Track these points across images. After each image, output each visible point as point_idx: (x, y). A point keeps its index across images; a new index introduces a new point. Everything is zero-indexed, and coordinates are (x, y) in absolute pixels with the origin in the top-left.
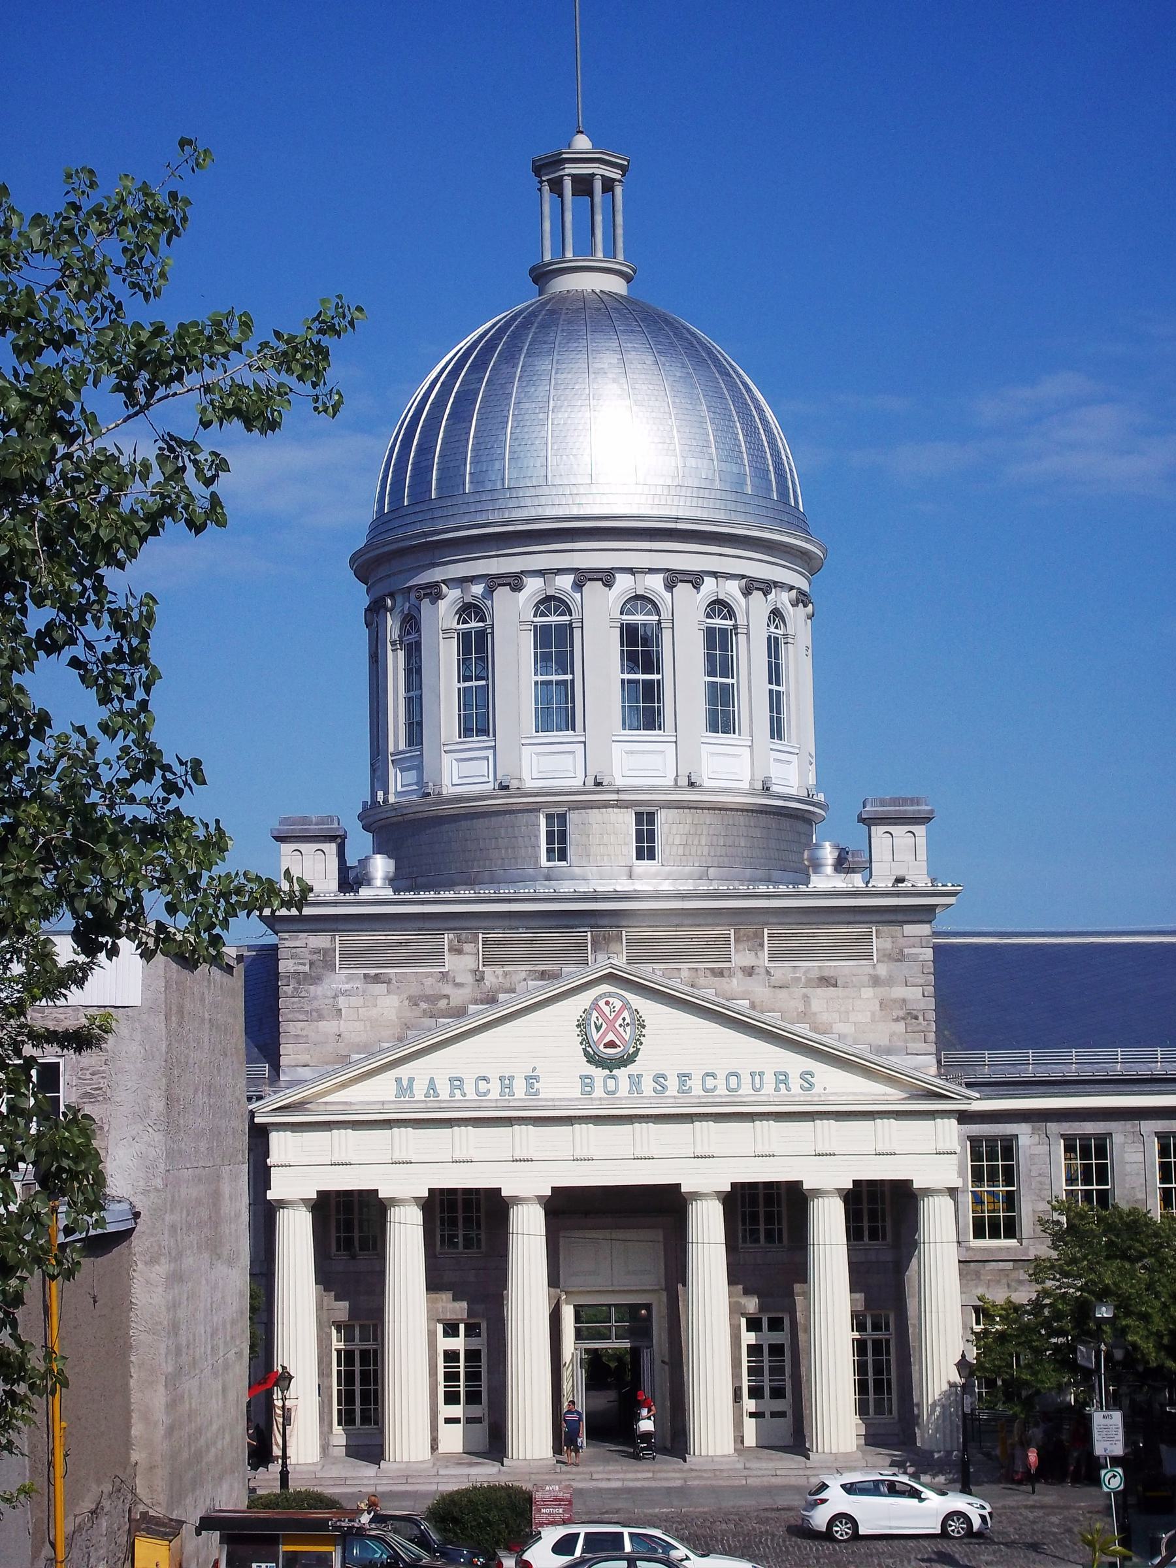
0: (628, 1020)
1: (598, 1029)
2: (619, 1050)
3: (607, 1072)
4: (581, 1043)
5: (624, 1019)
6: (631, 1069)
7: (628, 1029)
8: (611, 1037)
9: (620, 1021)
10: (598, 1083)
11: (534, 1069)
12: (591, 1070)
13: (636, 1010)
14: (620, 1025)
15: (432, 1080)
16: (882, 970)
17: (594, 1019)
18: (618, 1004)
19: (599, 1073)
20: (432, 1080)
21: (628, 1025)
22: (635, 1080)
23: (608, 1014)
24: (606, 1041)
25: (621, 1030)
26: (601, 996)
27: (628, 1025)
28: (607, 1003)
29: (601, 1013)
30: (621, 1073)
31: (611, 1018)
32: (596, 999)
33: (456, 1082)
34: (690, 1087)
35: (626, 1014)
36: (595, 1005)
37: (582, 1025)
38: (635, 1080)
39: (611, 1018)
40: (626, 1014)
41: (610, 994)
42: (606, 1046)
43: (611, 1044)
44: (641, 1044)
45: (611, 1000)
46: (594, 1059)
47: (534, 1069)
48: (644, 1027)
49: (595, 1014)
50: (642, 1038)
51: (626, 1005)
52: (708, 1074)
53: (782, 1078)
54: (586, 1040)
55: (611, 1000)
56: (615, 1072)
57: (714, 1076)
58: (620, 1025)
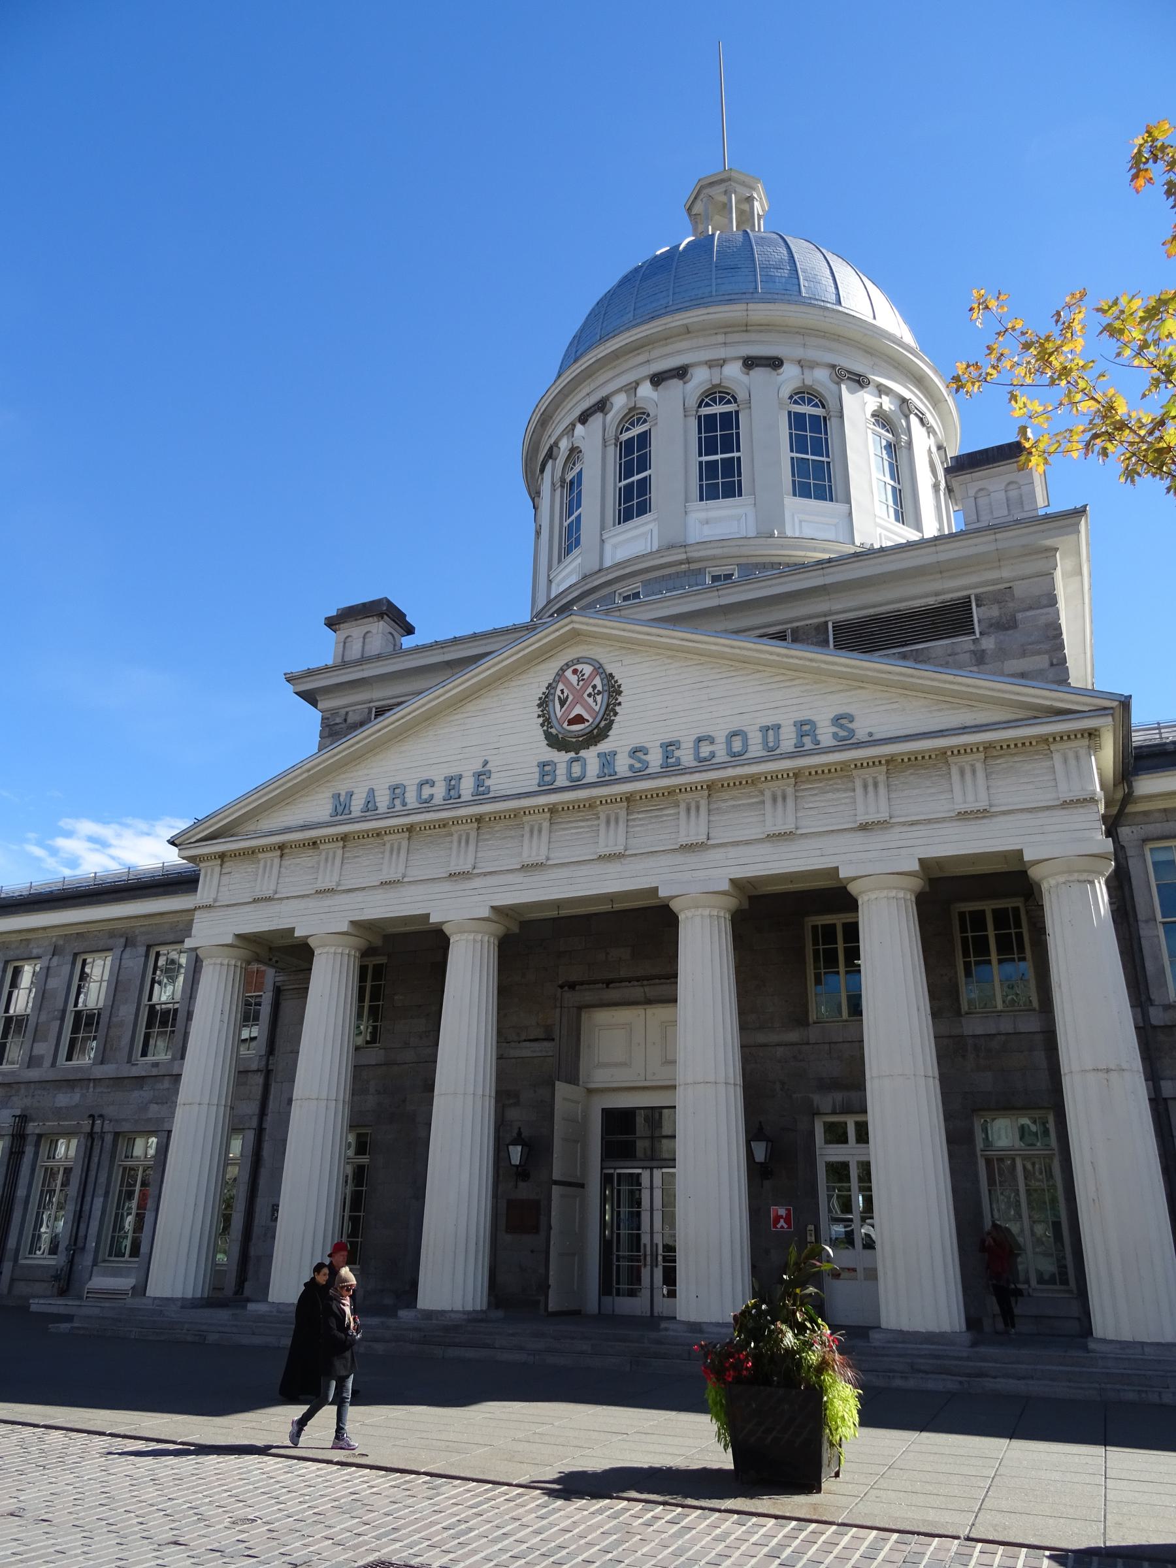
0: (599, 688)
1: (563, 703)
2: (587, 724)
3: (572, 754)
4: (542, 725)
5: (594, 687)
6: (604, 746)
7: (599, 698)
8: (578, 710)
9: (590, 690)
10: (561, 770)
11: (486, 763)
13: (611, 675)
14: (589, 695)
15: (372, 791)
16: (988, 643)
17: (558, 693)
18: (587, 670)
19: (561, 758)
20: (372, 791)
21: (599, 693)
22: (607, 760)
23: (575, 683)
24: (572, 716)
25: (590, 700)
26: (567, 665)
27: (599, 693)
28: (575, 672)
29: (568, 683)
30: (590, 755)
31: (578, 688)
32: (563, 670)
33: (397, 791)
34: (678, 758)
35: (597, 681)
36: (560, 675)
37: (544, 703)
38: (607, 760)
39: (578, 688)
41: (579, 661)
42: (571, 722)
43: (579, 719)
44: (616, 714)
45: (579, 667)
46: (556, 742)
47: (486, 763)
48: (620, 693)
49: (561, 686)
50: (617, 708)
51: (599, 669)
52: (699, 740)
53: (805, 728)
54: (547, 722)
55: (579, 667)
56: (583, 753)
57: (711, 740)
58: (589, 695)
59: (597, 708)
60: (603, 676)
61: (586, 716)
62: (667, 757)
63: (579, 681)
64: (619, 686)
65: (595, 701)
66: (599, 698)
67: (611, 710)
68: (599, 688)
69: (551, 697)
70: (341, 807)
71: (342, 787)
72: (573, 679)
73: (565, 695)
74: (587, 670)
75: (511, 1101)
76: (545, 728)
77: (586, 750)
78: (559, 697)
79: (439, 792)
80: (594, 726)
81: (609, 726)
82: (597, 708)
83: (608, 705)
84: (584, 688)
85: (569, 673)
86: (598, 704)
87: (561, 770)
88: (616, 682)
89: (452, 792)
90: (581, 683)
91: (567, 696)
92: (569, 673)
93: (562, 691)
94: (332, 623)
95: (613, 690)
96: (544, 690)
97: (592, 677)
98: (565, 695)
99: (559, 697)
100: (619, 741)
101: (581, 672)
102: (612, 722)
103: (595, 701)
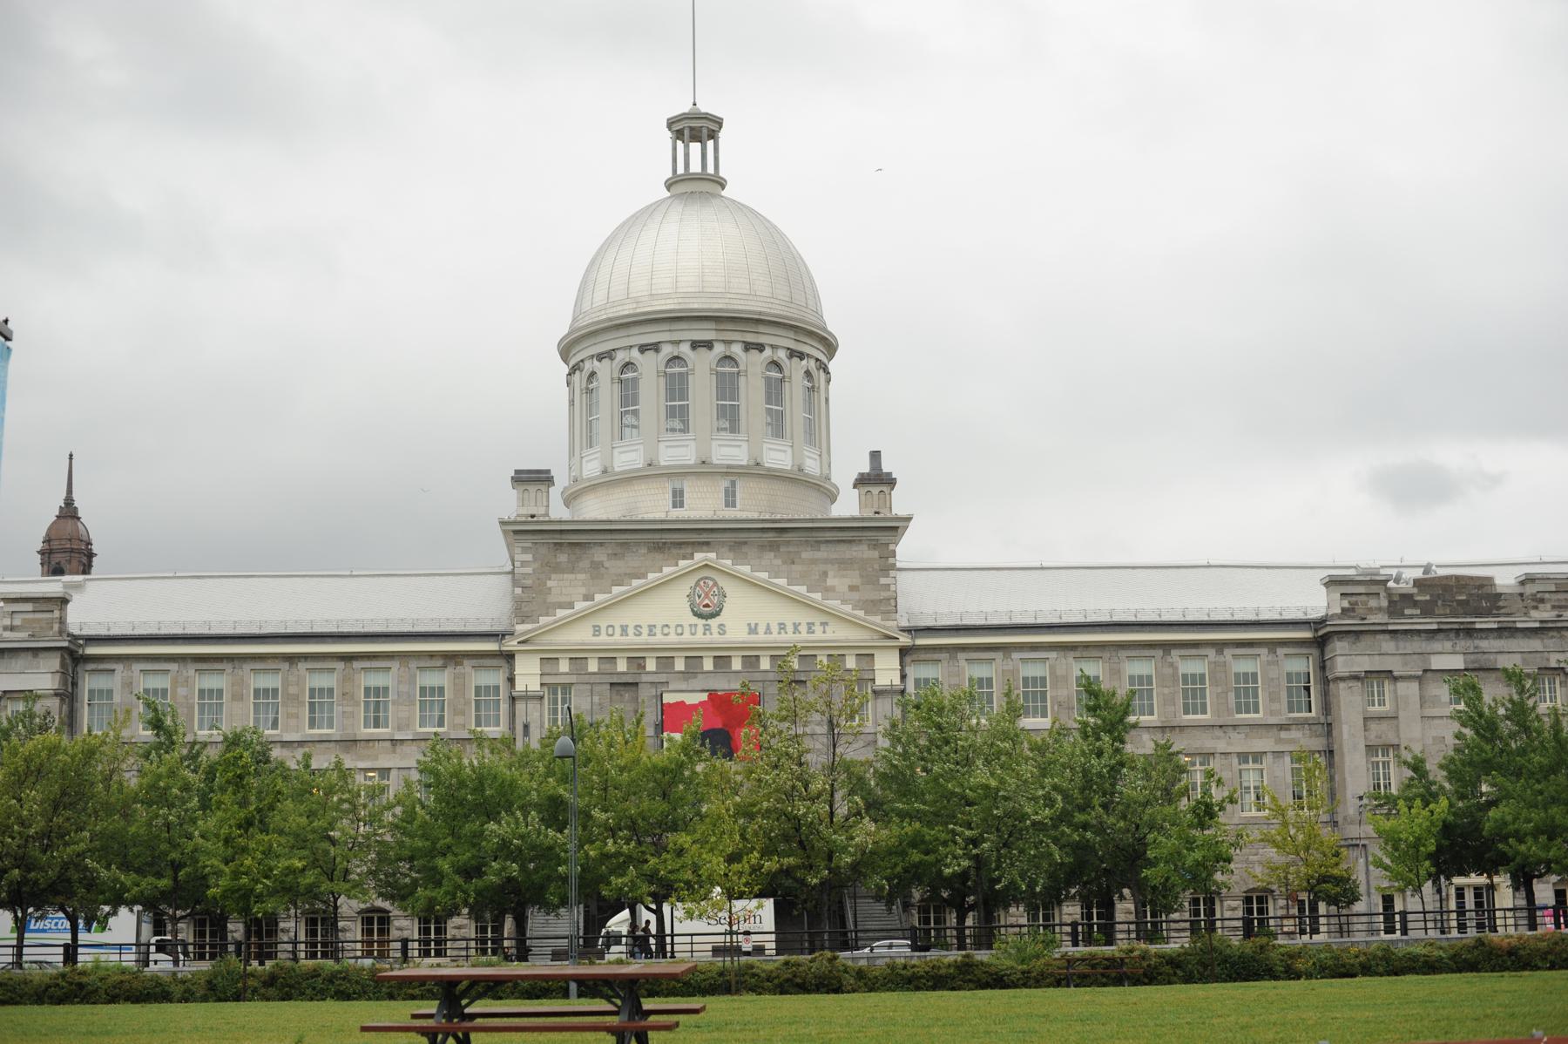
1: (699, 597)
8: (707, 601)
12: (695, 620)
18: (711, 583)
19: (701, 622)
26: (702, 579)
30: (714, 622)
35: (715, 589)
36: (697, 584)
40: (715, 589)
41: (706, 578)
43: (707, 606)
46: (696, 614)
51: (715, 584)
74: (711, 583)
81: (721, 610)
84: (710, 591)
85: (702, 583)
87: (700, 629)
92: (702, 583)
97: (713, 586)
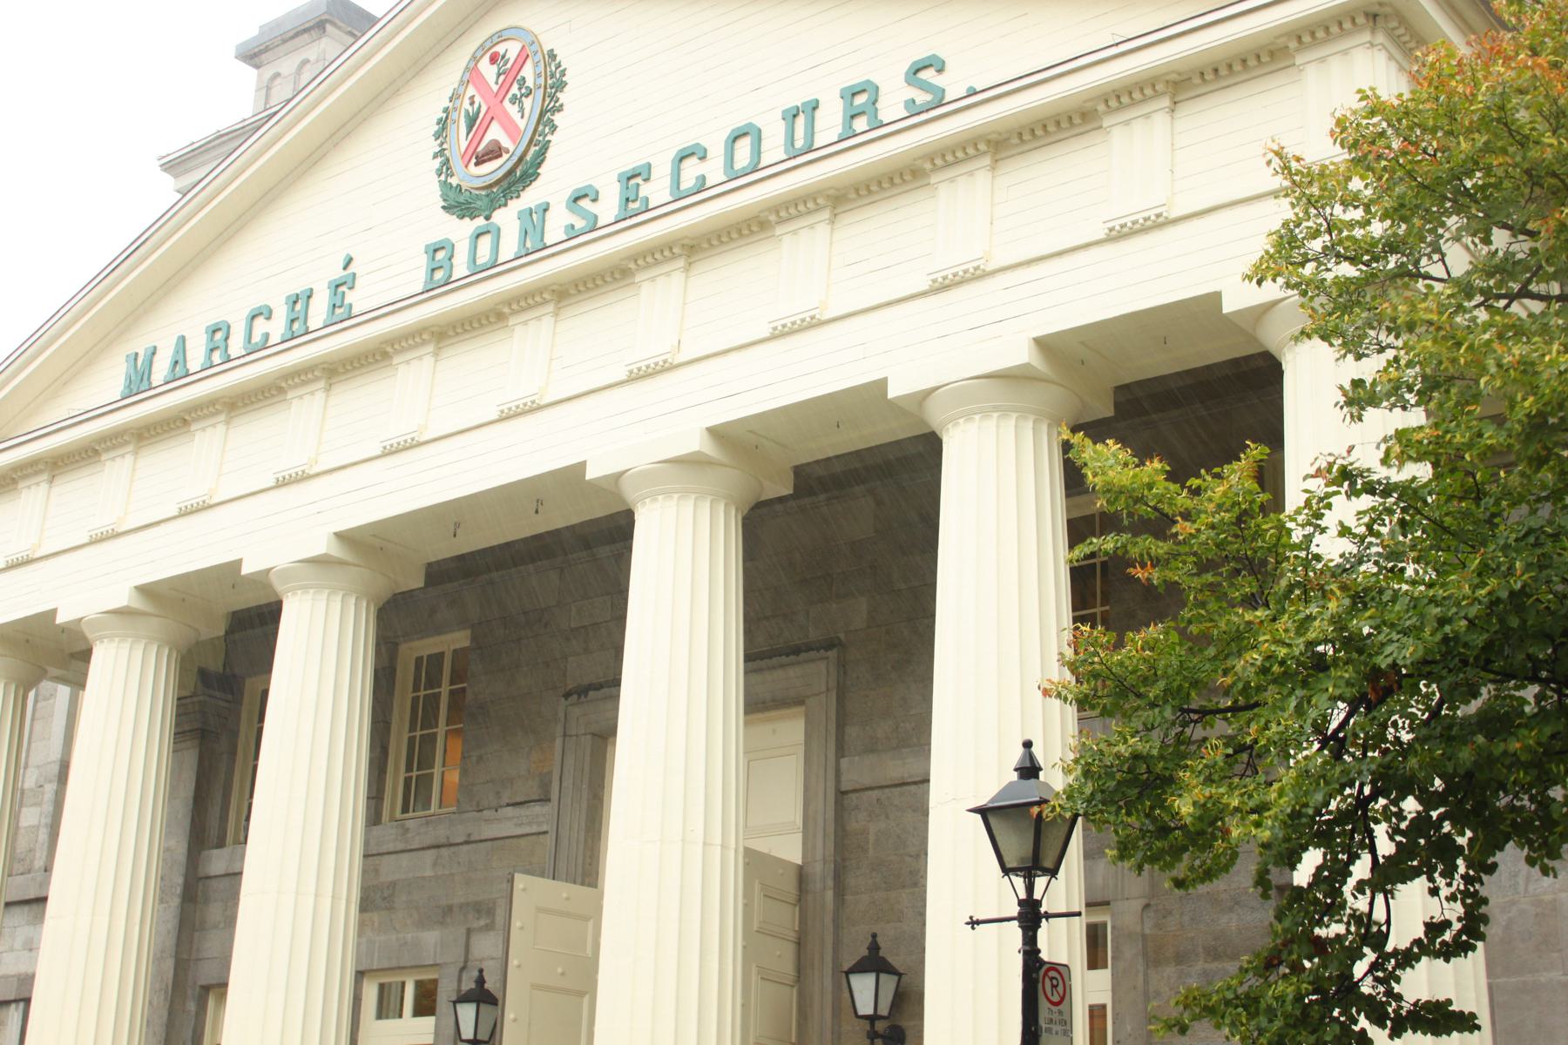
2: (505, 156)
3: (480, 221)
6: (531, 197)
7: (527, 102)
8: (495, 133)
11: (349, 262)
14: (514, 100)
15: (182, 340)
19: (460, 230)
22: (535, 220)
30: (507, 218)
32: (475, 59)
41: (501, 37)
43: (495, 152)
44: (554, 128)
45: (500, 49)
46: (460, 204)
47: (349, 262)
50: (558, 118)
59: (522, 127)
60: (539, 56)
61: (506, 143)
62: (627, 199)
63: (499, 75)
64: (563, 73)
65: (522, 110)
66: (527, 102)
67: (545, 120)
68: (530, 83)
69: (454, 115)
70: (139, 383)
71: (140, 345)
72: (489, 71)
73: (476, 106)
75: (482, 923)
76: (443, 178)
77: (503, 210)
78: (467, 111)
79: (276, 328)
80: (515, 159)
82: (522, 124)
83: (542, 115)
86: (522, 117)
88: (559, 66)
89: (296, 326)
90: (502, 78)
91: (480, 106)
93: (472, 98)
94: (253, 55)
95: (555, 83)
96: (447, 104)
98: (476, 106)
99: (467, 111)
100: (550, 187)
101: (504, 57)
102: (545, 147)
103: (522, 110)
